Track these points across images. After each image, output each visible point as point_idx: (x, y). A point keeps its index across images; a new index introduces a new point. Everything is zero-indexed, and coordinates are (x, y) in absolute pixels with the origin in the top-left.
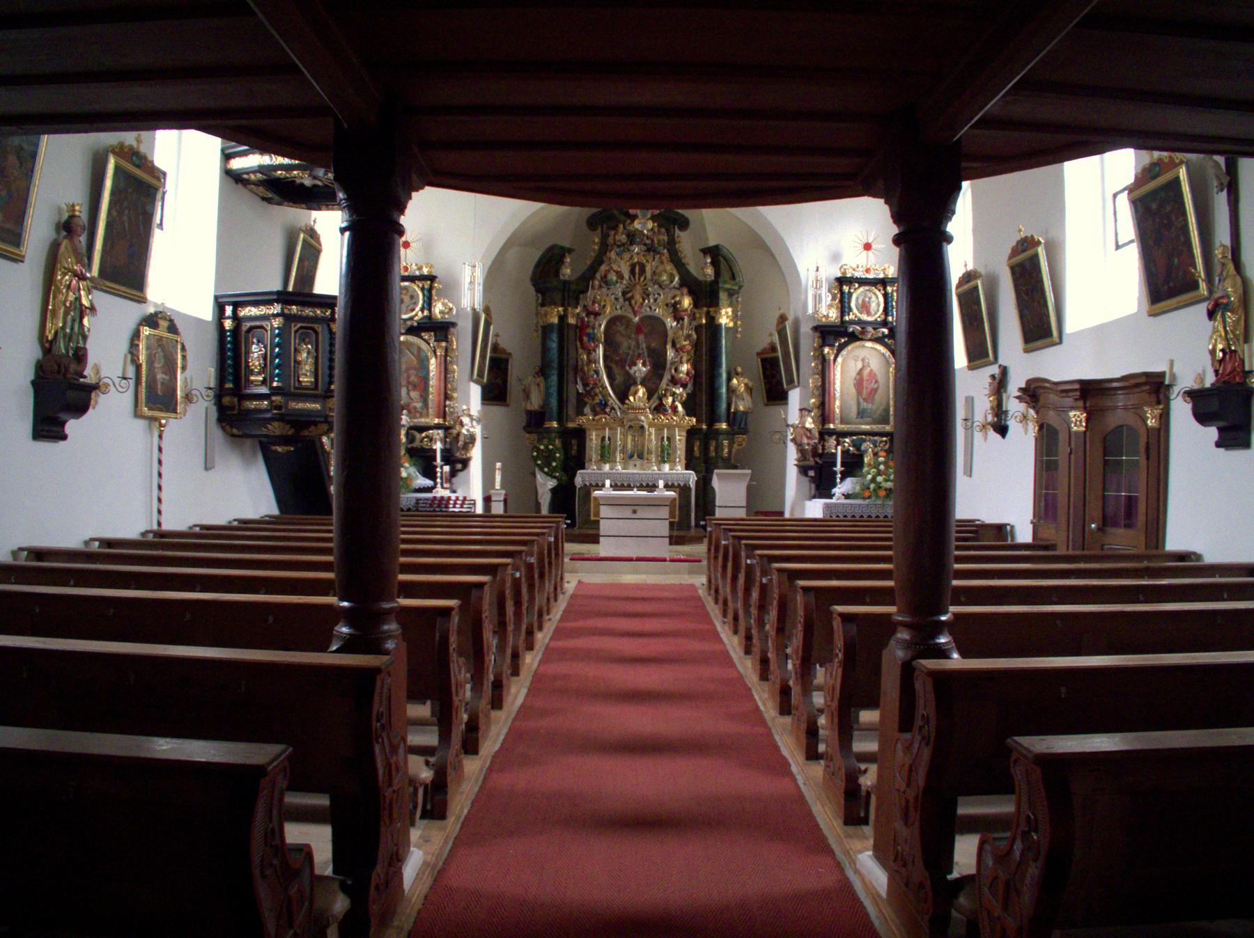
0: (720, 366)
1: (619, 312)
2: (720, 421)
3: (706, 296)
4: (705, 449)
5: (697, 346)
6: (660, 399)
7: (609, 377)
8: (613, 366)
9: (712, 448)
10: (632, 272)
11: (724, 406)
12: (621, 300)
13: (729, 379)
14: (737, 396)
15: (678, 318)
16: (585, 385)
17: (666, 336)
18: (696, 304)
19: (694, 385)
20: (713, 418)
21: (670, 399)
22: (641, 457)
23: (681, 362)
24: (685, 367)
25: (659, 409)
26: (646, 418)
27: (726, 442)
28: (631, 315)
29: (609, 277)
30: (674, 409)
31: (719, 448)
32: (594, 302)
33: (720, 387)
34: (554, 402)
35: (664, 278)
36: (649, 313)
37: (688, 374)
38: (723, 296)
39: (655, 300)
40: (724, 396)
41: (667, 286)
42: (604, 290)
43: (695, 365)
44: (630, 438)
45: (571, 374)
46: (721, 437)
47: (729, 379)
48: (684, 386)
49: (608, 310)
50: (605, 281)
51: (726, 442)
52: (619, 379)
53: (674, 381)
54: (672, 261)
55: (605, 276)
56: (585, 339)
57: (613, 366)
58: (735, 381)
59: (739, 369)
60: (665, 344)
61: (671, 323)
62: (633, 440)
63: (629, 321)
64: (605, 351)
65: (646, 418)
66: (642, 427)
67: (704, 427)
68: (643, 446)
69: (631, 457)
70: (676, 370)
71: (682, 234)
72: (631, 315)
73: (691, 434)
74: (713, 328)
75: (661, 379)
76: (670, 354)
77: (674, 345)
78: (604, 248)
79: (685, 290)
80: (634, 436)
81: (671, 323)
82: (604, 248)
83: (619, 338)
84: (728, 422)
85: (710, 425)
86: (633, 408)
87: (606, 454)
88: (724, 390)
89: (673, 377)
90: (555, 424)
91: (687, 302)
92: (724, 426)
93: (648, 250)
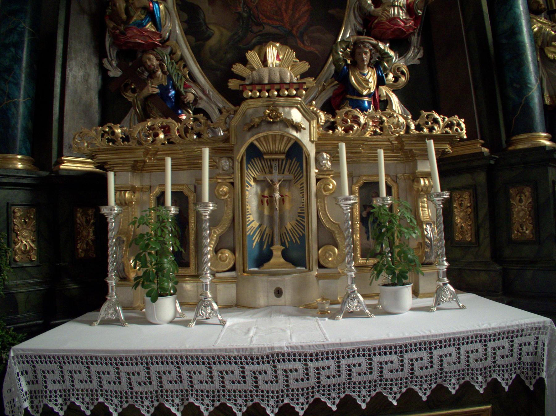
6: (341, 77)
7: (187, 32)
19: (427, 44)
21: (371, 76)
22: (296, 257)
25: (341, 97)
26: (304, 124)
44: (252, 192)
48: (400, 44)
52: (218, 36)
62: (267, 200)
65: (304, 124)
66: (296, 150)
68: (302, 217)
69: (263, 258)
80: (266, 186)
86: (258, 84)
87: (173, 256)
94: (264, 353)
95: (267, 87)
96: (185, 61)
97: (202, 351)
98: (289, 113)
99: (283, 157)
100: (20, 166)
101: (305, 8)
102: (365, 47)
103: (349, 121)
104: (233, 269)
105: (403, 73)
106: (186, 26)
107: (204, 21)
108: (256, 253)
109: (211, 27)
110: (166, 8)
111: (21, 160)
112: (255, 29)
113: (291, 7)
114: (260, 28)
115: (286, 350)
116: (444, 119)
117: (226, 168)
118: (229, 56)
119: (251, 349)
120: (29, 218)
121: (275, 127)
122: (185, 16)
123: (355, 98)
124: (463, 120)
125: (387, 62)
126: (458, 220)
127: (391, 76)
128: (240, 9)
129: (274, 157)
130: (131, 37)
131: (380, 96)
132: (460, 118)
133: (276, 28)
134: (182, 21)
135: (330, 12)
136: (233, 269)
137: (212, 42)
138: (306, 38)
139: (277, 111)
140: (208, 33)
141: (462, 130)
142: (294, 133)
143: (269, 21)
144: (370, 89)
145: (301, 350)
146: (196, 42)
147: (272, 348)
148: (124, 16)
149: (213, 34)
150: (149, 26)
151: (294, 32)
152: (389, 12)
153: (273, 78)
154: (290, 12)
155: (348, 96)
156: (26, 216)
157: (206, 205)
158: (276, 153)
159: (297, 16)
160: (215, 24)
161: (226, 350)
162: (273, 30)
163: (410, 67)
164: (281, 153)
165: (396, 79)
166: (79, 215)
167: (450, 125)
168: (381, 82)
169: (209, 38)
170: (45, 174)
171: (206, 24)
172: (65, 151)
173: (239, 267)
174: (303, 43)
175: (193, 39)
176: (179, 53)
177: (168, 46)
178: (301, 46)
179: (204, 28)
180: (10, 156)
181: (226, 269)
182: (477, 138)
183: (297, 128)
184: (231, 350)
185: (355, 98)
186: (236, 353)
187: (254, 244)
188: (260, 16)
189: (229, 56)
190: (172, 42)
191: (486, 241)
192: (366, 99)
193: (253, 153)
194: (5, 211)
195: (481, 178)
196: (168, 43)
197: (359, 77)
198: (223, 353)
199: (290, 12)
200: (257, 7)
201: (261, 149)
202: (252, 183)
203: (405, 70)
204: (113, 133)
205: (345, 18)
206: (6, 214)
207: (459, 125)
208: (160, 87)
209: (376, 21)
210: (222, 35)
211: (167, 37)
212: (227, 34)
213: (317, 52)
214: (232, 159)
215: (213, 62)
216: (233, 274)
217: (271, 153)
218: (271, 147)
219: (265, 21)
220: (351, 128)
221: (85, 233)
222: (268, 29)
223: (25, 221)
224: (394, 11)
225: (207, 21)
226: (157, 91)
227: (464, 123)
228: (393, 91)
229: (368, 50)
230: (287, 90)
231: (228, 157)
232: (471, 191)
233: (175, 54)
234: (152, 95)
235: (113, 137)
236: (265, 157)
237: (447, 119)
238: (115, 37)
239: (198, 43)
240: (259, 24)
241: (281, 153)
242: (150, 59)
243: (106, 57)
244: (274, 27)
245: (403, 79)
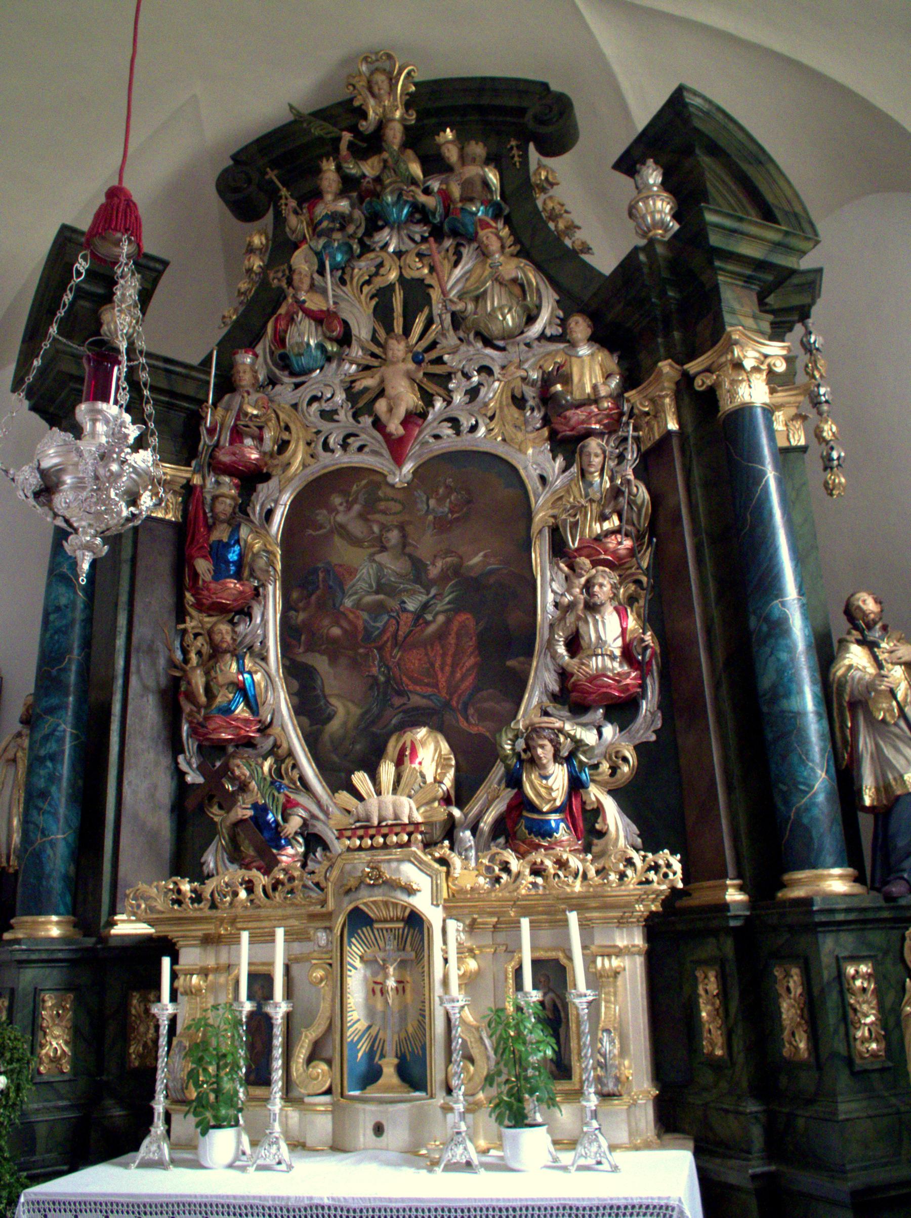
0: (770, 585)
1: (341, 459)
2: (810, 860)
3: (657, 312)
4: (753, 1010)
5: (656, 529)
8: (320, 663)
9: (789, 1010)
10: (383, 313)
11: (819, 779)
12: (344, 416)
13: (826, 652)
14: (879, 727)
15: (567, 445)
16: (213, 750)
17: (528, 515)
18: (632, 378)
19: (668, 705)
20: (773, 850)
21: (559, 777)
22: (413, 1076)
23: (592, 608)
24: (610, 629)
27: (860, 973)
28: (380, 462)
29: (292, 337)
30: (589, 828)
31: (825, 1006)
32: (237, 435)
33: (784, 688)
34: (59, 837)
35: (496, 299)
36: (450, 441)
37: (627, 654)
38: (738, 305)
39: (473, 393)
40: (814, 728)
41: (510, 335)
42: (285, 393)
43: (659, 602)
45: (145, 714)
46: (829, 946)
47: (826, 652)
48: (622, 710)
49: (298, 455)
50: (286, 363)
51: (860, 973)
52: (343, 714)
53: (573, 697)
54: (523, 253)
55: (280, 340)
56: (203, 566)
57: (320, 663)
58: (856, 657)
59: (869, 605)
60: (527, 546)
61: (534, 459)
63: (376, 479)
64: (288, 607)
66: (415, 920)
67: (734, 896)
68: (423, 1016)
69: (371, 1076)
70: (574, 644)
71: (560, 165)
72: (380, 462)
73: (672, 936)
74: (719, 433)
75: (517, 686)
76: (550, 589)
77: (559, 549)
78: (282, 247)
79: (580, 327)
81: (534, 459)
82: (282, 247)
83: (342, 553)
84: (851, 856)
85: (765, 881)
88: (808, 699)
89: (564, 675)
90: (53, 928)
91: (591, 371)
92: (836, 882)
93: (437, 234)
94: (302, 1204)
95: (372, 831)
96: (294, 759)
97: (235, 1197)
98: (398, 870)
99: (401, 925)
100: (55, 932)
101: (470, 662)
102: (539, 737)
103: (497, 869)
104: (329, 1092)
105: (625, 759)
106: (296, 700)
107: (323, 691)
108: (362, 1068)
109: (333, 701)
110: (268, 674)
111: (58, 923)
112: (397, 701)
113: (449, 660)
114: (404, 700)
115: (326, 1202)
116: (645, 857)
117: (323, 942)
118: (358, 747)
119: (288, 1198)
120: (64, 1008)
121: (376, 891)
122: (296, 685)
123: (536, 816)
124: (679, 857)
125: (584, 753)
126: (704, 1014)
127: (605, 767)
128: (375, 671)
129: (388, 926)
130: (214, 730)
131: (584, 803)
132: (673, 853)
133: (428, 697)
134: (290, 694)
135: (510, 663)
136: (329, 1092)
137: (335, 725)
138: (471, 711)
139: (378, 869)
140: (328, 711)
141: (675, 873)
142: (403, 898)
143: (418, 688)
144: (555, 800)
145: (343, 1204)
146: (311, 725)
147: (311, 1198)
148: (203, 699)
149: (335, 713)
150: (241, 710)
151: (454, 703)
152: (588, 666)
153: (384, 813)
154: (448, 669)
155: (525, 813)
156: (59, 1005)
157: (276, 1005)
158: (392, 920)
159: (458, 675)
160: (339, 696)
161: (260, 1198)
162: (423, 702)
163: (637, 748)
164: (398, 920)
165: (614, 769)
166: (135, 1002)
167: (656, 868)
168: (576, 785)
169: (330, 718)
170: (90, 942)
171: (325, 697)
172: (119, 907)
173: (337, 1089)
174: (467, 720)
175: (305, 720)
176: (285, 745)
177: (270, 735)
178: (464, 724)
179: (322, 703)
180: (42, 919)
181: (320, 1091)
182: (726, 876)
183: (410, 891)
184: (265, 1198)
185: (536, 816)
186: (270, 1203)
187: (360, 1055)
188: (404, 679)
189: (358, 747)
190: (276, 730)
191: (740, 1058)
192: (553, 817)
193: (358, 920)
194: (31, 1000)
195: (729, 946)
196: (269, 731)
197: (537, 782)
198: (257, 1202)
199: (448, 669)
200: (398, 664)
201: (372, 915)
202: (358, 963)
203: (630, 754)
204: (179, 891)
205: (532, 674)
206: (32, 1005)
207: (669, 865)
208: (255, 806)
209: (573, 680)
210: (348, 713)
211: (269, 719)
212: (356, 711)
213: (487, 734)
214: (329, 929)
215: (336, 759)
216: (327, 1099)
217: (385, 921)
218: (384, 913)
219: (410, 687)
220: (498, 879)
221: (142, 1029)
222: (416, 700)
223: (58, 1014)
224: (596, 663)
225: (327, 691)
226: (250, 813)
227: (680, 861)
228: (611, 792)
229: (546, 742)
230: (397, 834)
231: (326, 928)
232: (717, 967)
233: (279, 747)
234: (242, 822)
235: (180, 897)
236: (376, 925)
237: (650, 855)
238: (194, 731)
239: (315, 727)
240: (400, 693)
241: (398, 920)
242: (238, 766)
243: (182, 751)
244: (424, 697)
245: (626, 769)
